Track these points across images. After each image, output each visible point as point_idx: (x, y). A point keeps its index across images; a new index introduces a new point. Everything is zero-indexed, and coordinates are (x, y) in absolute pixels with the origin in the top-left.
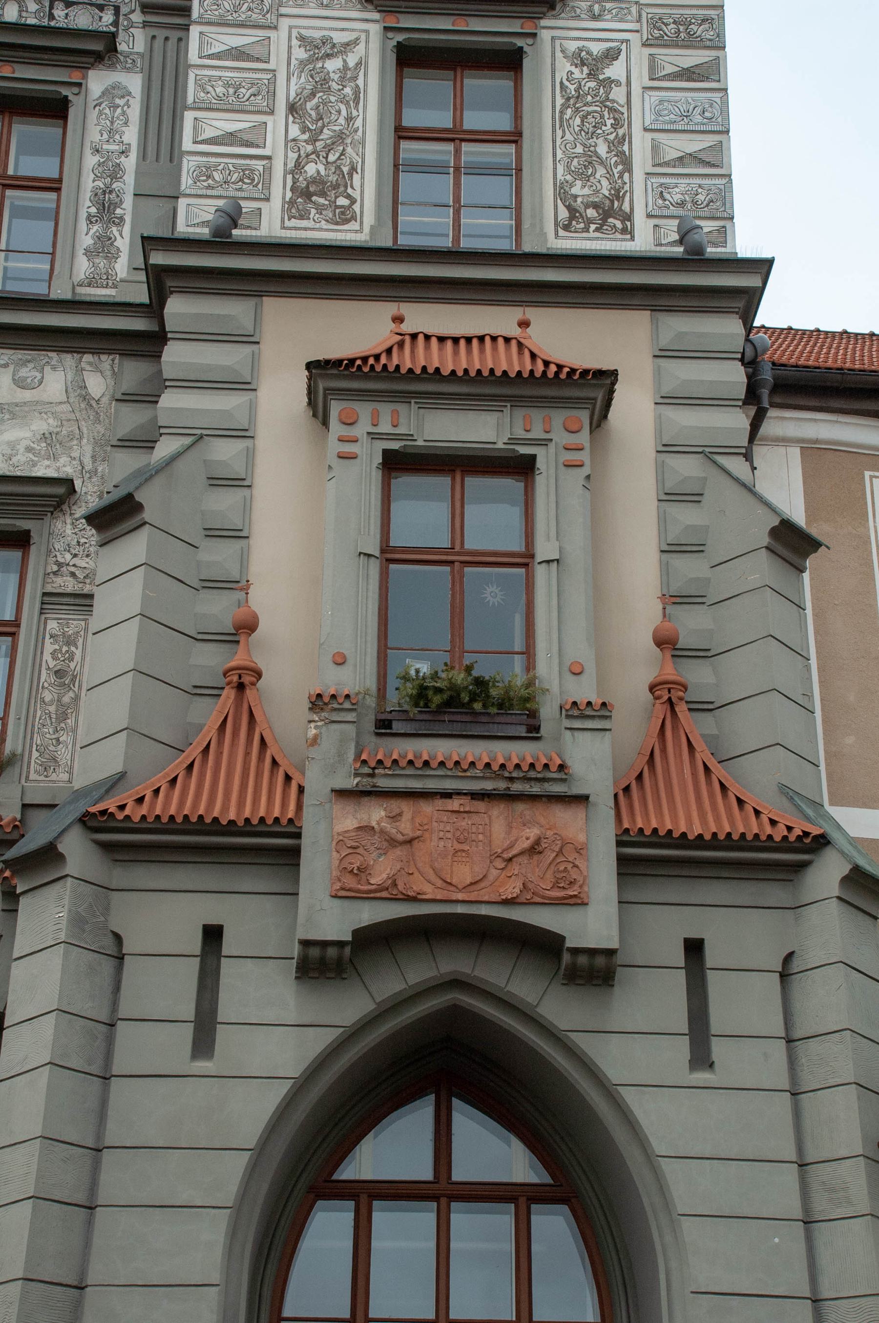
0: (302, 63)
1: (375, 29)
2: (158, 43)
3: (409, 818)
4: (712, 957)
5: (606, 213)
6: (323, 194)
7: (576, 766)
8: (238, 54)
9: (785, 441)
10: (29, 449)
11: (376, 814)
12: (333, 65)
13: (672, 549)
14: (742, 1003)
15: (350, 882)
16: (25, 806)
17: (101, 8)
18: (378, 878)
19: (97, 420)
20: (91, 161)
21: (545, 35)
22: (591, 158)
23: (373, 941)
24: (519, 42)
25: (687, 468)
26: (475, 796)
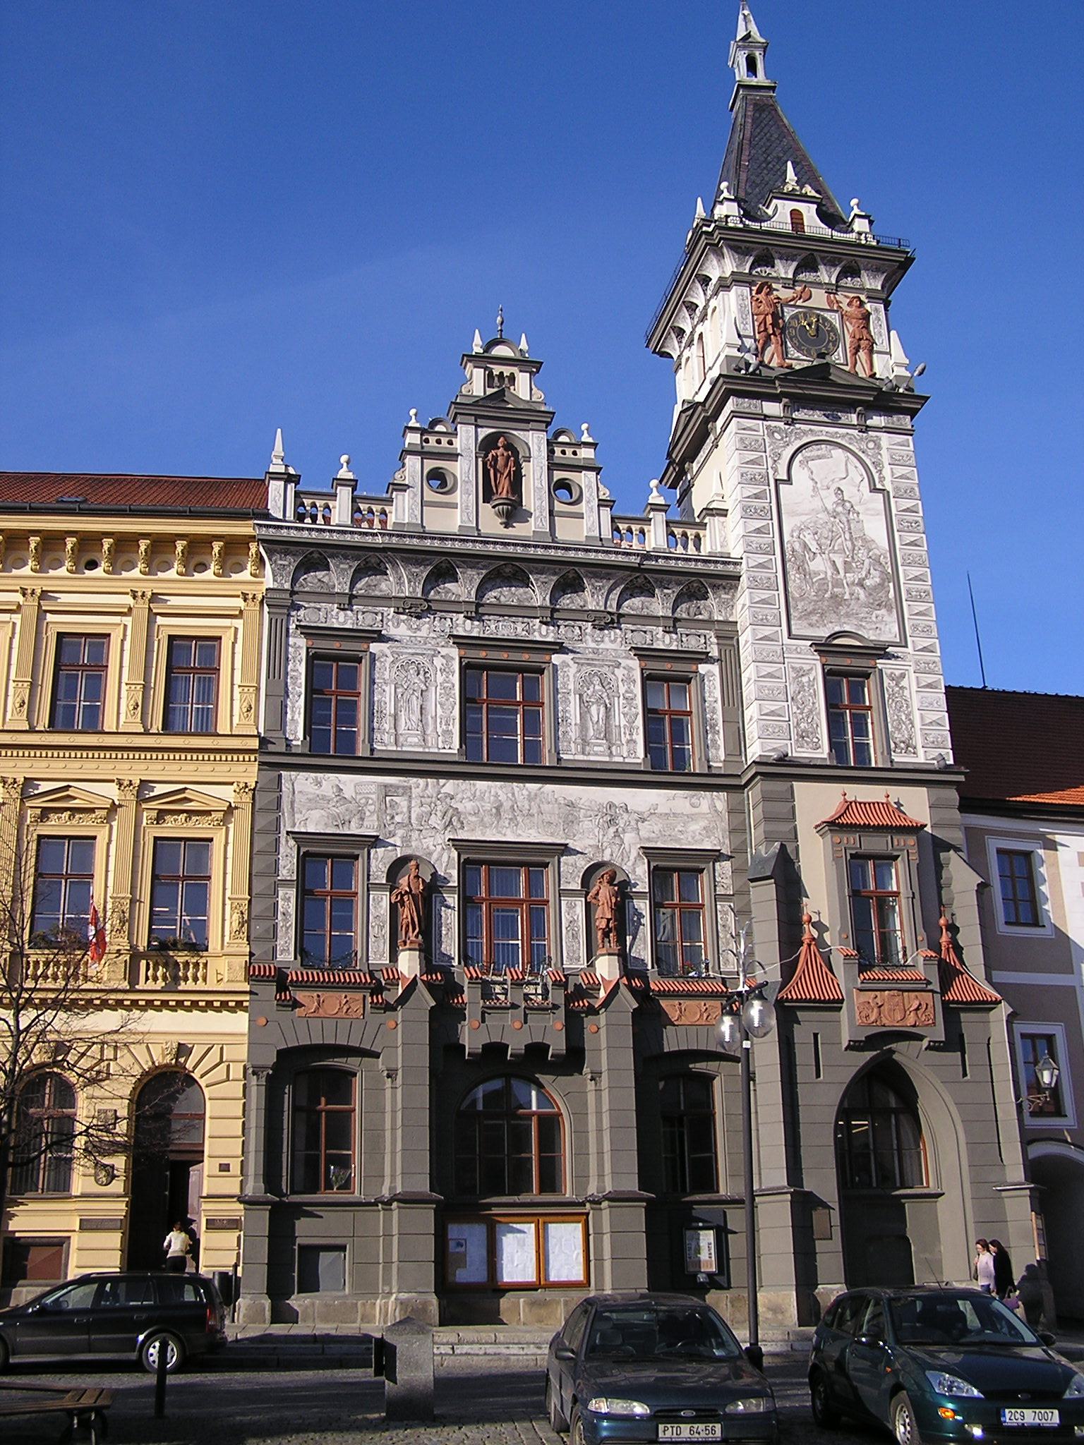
5: (908, 746)
12: (805, 679)
18: (872, 1019)
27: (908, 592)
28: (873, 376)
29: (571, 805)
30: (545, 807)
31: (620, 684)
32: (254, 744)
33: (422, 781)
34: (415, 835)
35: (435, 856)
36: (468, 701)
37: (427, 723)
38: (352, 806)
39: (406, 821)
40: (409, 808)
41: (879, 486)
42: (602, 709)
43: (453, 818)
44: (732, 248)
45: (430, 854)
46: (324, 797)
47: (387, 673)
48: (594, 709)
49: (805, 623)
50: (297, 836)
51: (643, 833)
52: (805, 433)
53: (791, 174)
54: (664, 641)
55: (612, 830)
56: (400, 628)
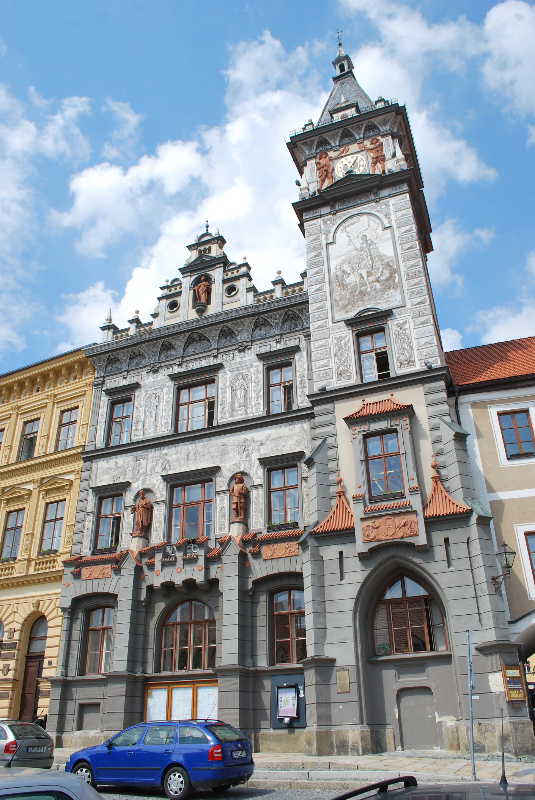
0: (336, 344)
1: (351, 331)
2: (308, 343)
3: (377, 522)
4: (451, 542)
5: (409, 362)
6: (344, 373)
7: (412, 503)
8: (322, 346)
9: (466, 403)
10: (294, 445)
11: (369, 523)
12: (342, 342)
14: (458, 550)
15: (367, 539)
16: (305, 527)
17: (296, 339)
18: (372, 537)
19: (307, 435)
21: (389, 322)
22: (404, 349)
23: (373, 552)
24: (383, 326)
26: (391, 515)
27: (408, 275)
29: (225, 445)
30: (212, 449)
31: (253, 375)
32: (80, 450)
34: (148, 478)
35: (156, 487)
37: (158, 421)
38: (121, 470)
39: (145, 472)
40: (147, 464)
41: (387, 225)
42: (243, 391)
43: (167, 464)
44: (303, 144)
45: (154, 486)
46: (110, 469)
47: (142, 402)
48: (238, 393)
49: (343, 312)
50: (96, 490)
52: (344, 215)
55: (246, 453)
56: (148, 380)
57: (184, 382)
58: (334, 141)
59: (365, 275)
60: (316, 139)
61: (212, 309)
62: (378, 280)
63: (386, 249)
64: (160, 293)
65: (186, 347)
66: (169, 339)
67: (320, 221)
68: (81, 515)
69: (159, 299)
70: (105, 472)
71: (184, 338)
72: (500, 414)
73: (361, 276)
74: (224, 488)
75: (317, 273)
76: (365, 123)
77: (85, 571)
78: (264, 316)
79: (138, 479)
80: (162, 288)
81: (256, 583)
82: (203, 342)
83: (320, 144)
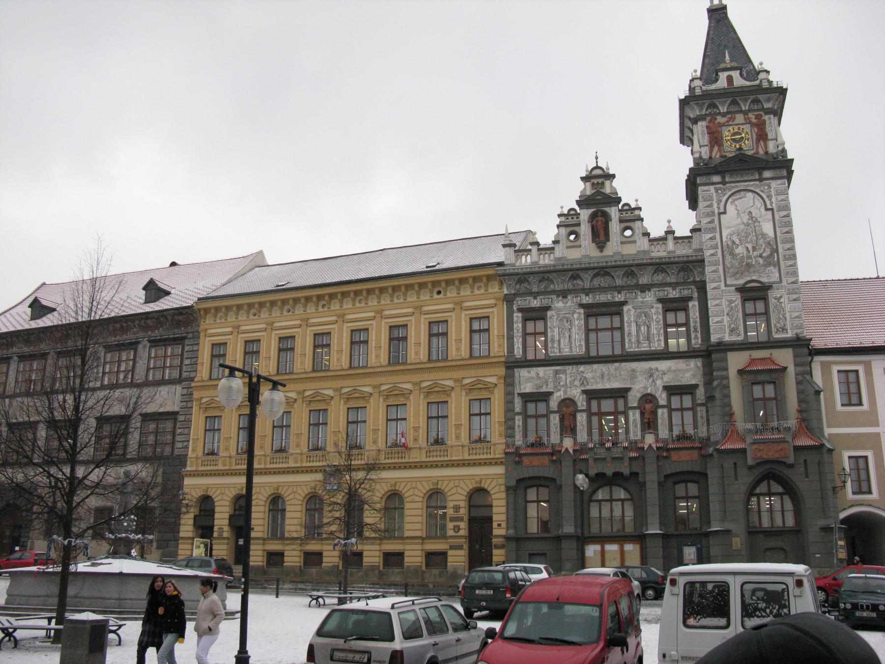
3: (761, 447)
8: (717, 305)
13: (798, 393)
20: (691, 320)
23: (758, 464)
25: (800, 378)
27: (785, 256)
28: (766, 153)
29: (633, 370)
30: (622, 373)
33: (571, 367)
34: (569, 389)
36: (588, 330)
41: (769, 207)
46: (532, 378)
48: (642, 328)
50: (523, 395)
51: (665, 379)
52: (733, 187)
53: (727, 57)
54: (673, 294)
56: (559, 304)
57: (592, 311)
58: (723, 106)
59: (750, 249)
60: (707, 103)
61: (613, 247)
62: (761, 256)
63: (767, 228)
64: (557, 221)
65: (592, 280)
66: (580, 273)
67: (712, 188)
68: (510, 414)
69: (558, 226)
70: (528, 380)
71: (592, 273)
72: (839, 371)
73: (747, 248)
74: (635, 405)
75: (711, 239)
76: (752, 97)
77: (525, 460)
78: (664, 266)
79: (559, 390)
80: (559, 216)
81: (667, 476)
82: (607, 277)
83: (709, 107)
